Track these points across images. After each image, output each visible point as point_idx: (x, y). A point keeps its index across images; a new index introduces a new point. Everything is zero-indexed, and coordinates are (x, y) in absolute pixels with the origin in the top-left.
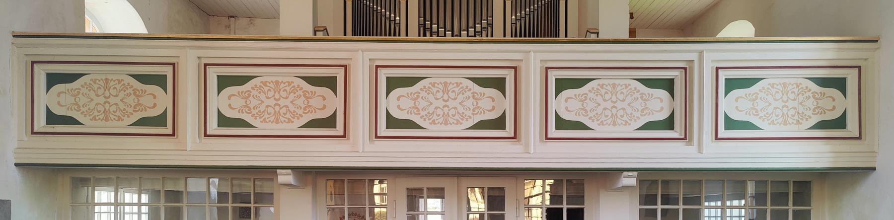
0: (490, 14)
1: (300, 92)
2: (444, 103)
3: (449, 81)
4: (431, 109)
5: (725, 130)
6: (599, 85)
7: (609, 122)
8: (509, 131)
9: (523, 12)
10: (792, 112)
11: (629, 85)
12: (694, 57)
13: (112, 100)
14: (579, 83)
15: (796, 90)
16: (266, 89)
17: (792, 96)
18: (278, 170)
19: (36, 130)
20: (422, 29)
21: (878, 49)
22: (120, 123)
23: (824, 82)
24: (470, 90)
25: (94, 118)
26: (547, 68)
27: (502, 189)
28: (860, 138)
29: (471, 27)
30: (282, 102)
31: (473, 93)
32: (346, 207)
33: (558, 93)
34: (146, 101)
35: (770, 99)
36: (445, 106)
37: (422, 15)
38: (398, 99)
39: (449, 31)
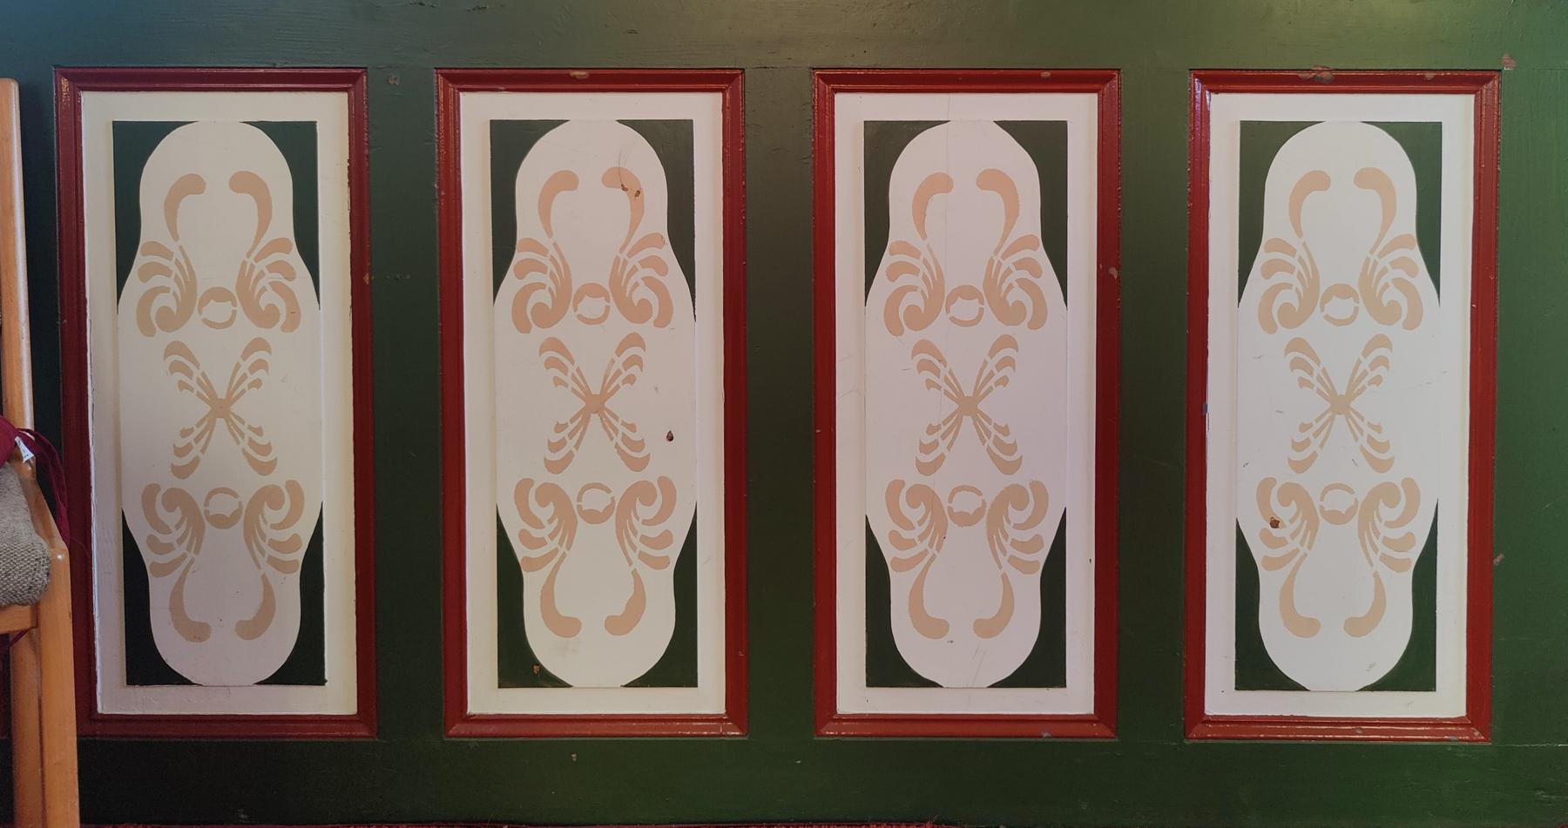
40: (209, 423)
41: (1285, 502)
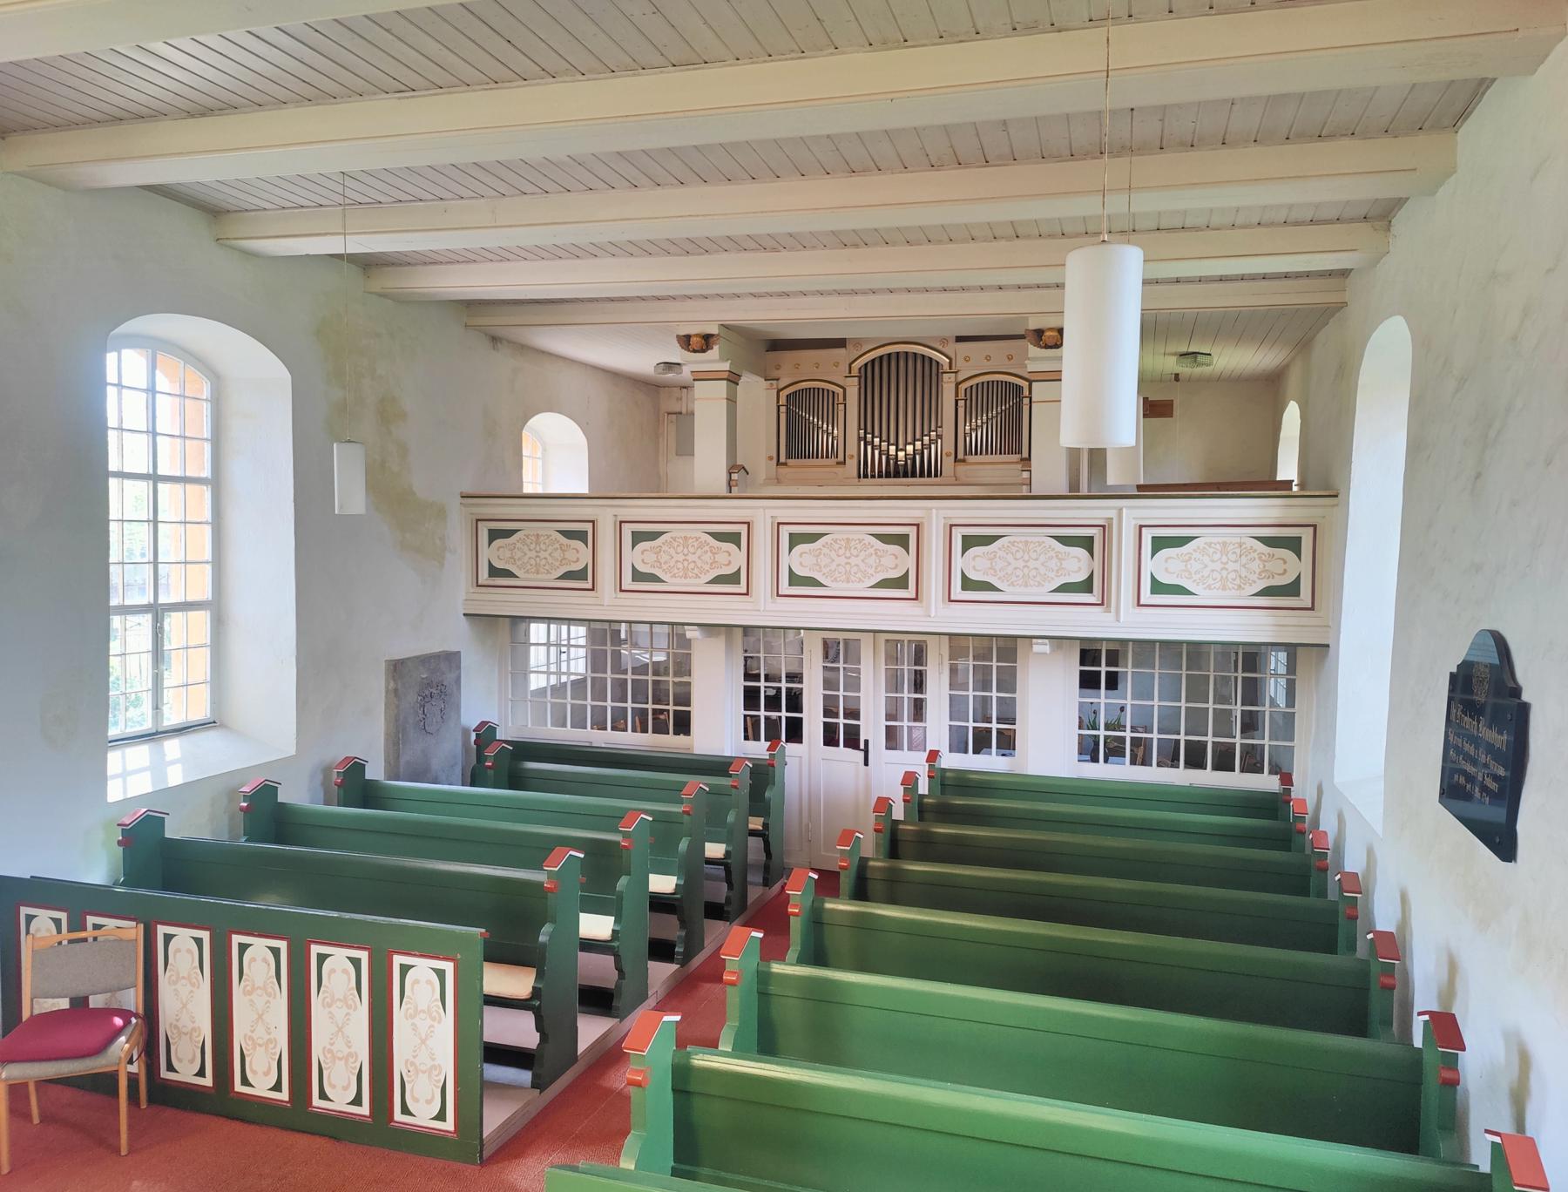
0: (939, 424)
1: (707, 548)
2: (846, 561)
3: (851, 537)
4: (833, 567)
5: (1152, 593)
6: (1010, 542)
7: (1020, 582)
9: (979, 421)
10: (1233, 575)
11: (1043, 542)
12: (1112, 514)
14: (988, 540)
15: (1238, 551)
16: (676, 544)
17: (1233, 557)
18: (686, 627)
19: (480, 583)
20: (862, 443)
21: (1337, 505)
23: (1270, 542)
24: (872, 546)
26: (951, 526)
28: (1312, 609)
29: (918, 440)
30: (690, 558)
31: (876, 550)
33: (964, 551)
34: (571, 555)
35: (1206, 559)
36: (847, 563)
37: (862, 426)
38: (801, 555)
39: (893, 445)
41: (411, 1066)
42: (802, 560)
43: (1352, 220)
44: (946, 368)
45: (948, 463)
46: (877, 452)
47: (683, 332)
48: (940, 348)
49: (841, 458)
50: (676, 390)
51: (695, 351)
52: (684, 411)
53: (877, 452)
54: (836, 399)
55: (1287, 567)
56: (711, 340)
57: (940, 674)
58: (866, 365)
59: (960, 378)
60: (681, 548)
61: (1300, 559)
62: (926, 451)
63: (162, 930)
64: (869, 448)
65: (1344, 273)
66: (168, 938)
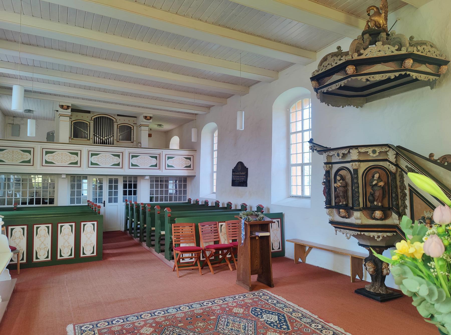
3: (106, 155)
8: (121, 166)
9: (122, 133)
12: (161, 152)
13: (14, 156)
18: (62, 175)
20: (94, 136)
22: (17, 162)
23: (186, 158)
25: (9, 161)
26: (130, 153)
27: (118, 179)
30: (63, 158)
32: (76, 183)
33: (132, 158)
36: (105, 160)
37: (94, 132)
40: (17, 245)
42: (94, 159)
43: (205, 107)
44: (115, 121)
45: (115, 142)
46: (97, 138)
47: (61, 104)
48: (114, 117)
49: (88, 139)
50: (12, 118)
51: (64, 109)
52: (15, 124)
53: (97, 138)
54: (87, 125)
55: (189, 163)
56: (69, 107)
57: (121, 185)
58: (95, 118)
59: (118, 124)
60: (60, 156)
61: (191, 161)
62: (110, 139)
63: (10, 228)
64: (96, 137)
65: (196, 114)
66: (12, 230)
